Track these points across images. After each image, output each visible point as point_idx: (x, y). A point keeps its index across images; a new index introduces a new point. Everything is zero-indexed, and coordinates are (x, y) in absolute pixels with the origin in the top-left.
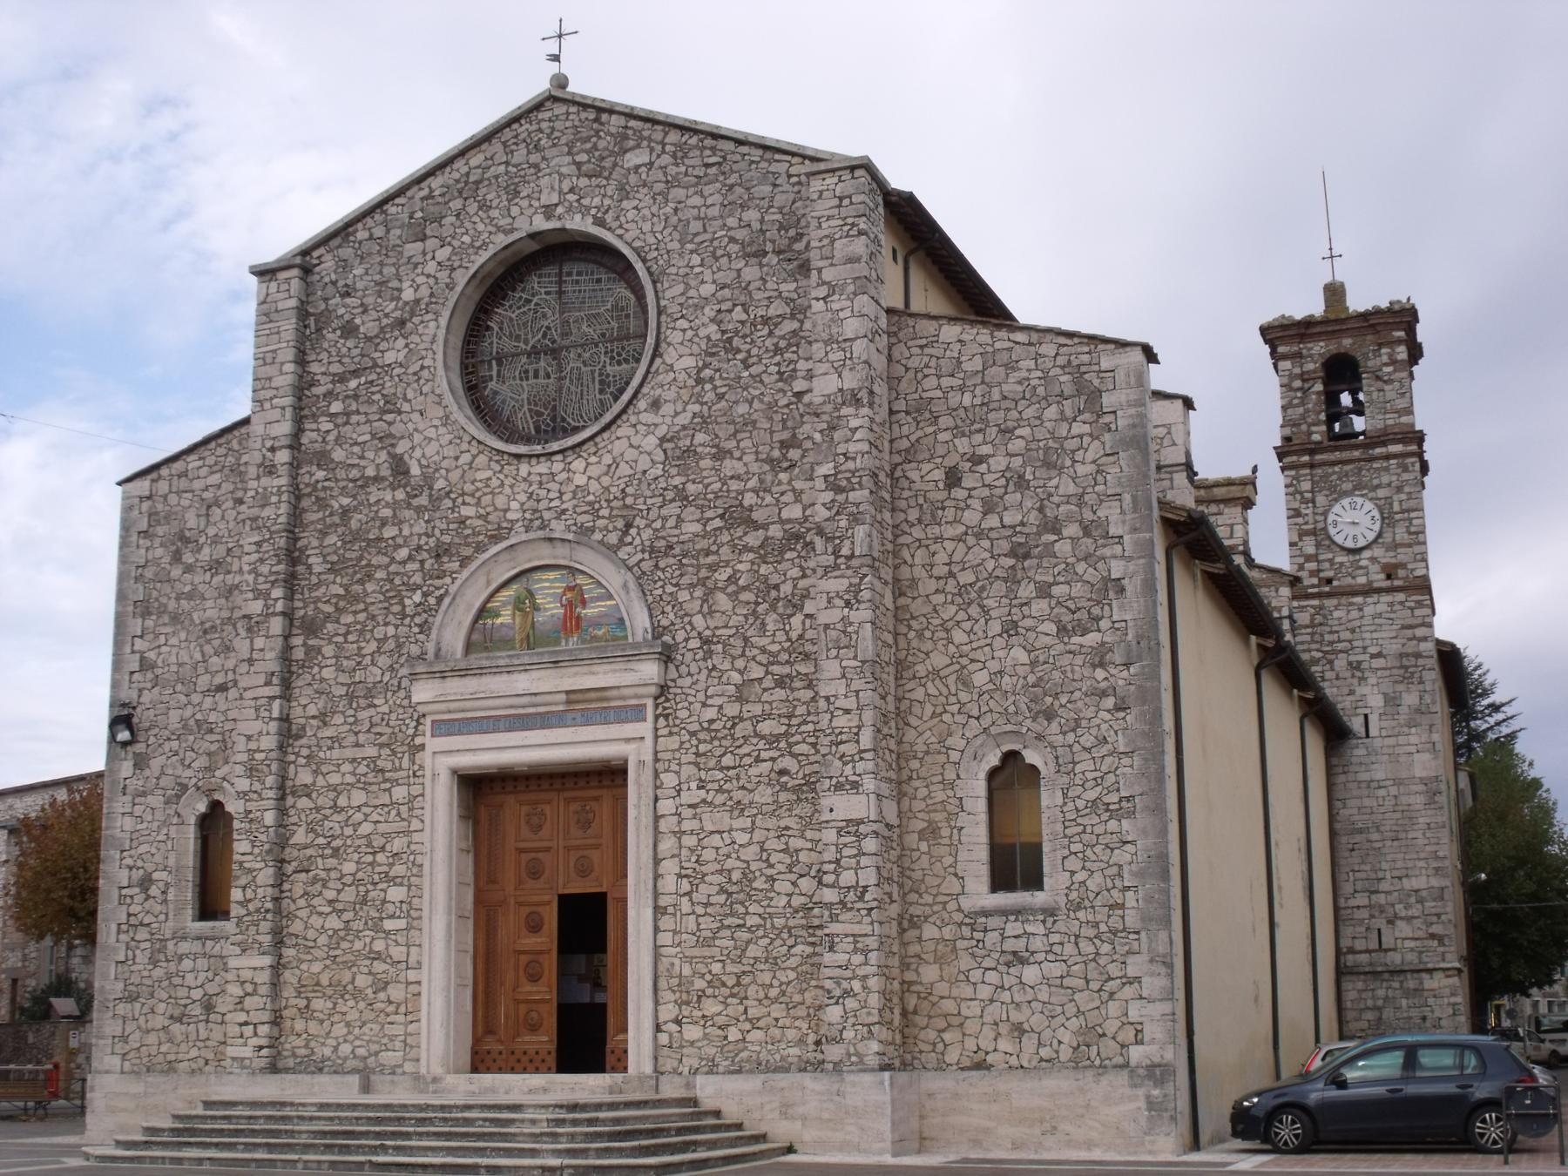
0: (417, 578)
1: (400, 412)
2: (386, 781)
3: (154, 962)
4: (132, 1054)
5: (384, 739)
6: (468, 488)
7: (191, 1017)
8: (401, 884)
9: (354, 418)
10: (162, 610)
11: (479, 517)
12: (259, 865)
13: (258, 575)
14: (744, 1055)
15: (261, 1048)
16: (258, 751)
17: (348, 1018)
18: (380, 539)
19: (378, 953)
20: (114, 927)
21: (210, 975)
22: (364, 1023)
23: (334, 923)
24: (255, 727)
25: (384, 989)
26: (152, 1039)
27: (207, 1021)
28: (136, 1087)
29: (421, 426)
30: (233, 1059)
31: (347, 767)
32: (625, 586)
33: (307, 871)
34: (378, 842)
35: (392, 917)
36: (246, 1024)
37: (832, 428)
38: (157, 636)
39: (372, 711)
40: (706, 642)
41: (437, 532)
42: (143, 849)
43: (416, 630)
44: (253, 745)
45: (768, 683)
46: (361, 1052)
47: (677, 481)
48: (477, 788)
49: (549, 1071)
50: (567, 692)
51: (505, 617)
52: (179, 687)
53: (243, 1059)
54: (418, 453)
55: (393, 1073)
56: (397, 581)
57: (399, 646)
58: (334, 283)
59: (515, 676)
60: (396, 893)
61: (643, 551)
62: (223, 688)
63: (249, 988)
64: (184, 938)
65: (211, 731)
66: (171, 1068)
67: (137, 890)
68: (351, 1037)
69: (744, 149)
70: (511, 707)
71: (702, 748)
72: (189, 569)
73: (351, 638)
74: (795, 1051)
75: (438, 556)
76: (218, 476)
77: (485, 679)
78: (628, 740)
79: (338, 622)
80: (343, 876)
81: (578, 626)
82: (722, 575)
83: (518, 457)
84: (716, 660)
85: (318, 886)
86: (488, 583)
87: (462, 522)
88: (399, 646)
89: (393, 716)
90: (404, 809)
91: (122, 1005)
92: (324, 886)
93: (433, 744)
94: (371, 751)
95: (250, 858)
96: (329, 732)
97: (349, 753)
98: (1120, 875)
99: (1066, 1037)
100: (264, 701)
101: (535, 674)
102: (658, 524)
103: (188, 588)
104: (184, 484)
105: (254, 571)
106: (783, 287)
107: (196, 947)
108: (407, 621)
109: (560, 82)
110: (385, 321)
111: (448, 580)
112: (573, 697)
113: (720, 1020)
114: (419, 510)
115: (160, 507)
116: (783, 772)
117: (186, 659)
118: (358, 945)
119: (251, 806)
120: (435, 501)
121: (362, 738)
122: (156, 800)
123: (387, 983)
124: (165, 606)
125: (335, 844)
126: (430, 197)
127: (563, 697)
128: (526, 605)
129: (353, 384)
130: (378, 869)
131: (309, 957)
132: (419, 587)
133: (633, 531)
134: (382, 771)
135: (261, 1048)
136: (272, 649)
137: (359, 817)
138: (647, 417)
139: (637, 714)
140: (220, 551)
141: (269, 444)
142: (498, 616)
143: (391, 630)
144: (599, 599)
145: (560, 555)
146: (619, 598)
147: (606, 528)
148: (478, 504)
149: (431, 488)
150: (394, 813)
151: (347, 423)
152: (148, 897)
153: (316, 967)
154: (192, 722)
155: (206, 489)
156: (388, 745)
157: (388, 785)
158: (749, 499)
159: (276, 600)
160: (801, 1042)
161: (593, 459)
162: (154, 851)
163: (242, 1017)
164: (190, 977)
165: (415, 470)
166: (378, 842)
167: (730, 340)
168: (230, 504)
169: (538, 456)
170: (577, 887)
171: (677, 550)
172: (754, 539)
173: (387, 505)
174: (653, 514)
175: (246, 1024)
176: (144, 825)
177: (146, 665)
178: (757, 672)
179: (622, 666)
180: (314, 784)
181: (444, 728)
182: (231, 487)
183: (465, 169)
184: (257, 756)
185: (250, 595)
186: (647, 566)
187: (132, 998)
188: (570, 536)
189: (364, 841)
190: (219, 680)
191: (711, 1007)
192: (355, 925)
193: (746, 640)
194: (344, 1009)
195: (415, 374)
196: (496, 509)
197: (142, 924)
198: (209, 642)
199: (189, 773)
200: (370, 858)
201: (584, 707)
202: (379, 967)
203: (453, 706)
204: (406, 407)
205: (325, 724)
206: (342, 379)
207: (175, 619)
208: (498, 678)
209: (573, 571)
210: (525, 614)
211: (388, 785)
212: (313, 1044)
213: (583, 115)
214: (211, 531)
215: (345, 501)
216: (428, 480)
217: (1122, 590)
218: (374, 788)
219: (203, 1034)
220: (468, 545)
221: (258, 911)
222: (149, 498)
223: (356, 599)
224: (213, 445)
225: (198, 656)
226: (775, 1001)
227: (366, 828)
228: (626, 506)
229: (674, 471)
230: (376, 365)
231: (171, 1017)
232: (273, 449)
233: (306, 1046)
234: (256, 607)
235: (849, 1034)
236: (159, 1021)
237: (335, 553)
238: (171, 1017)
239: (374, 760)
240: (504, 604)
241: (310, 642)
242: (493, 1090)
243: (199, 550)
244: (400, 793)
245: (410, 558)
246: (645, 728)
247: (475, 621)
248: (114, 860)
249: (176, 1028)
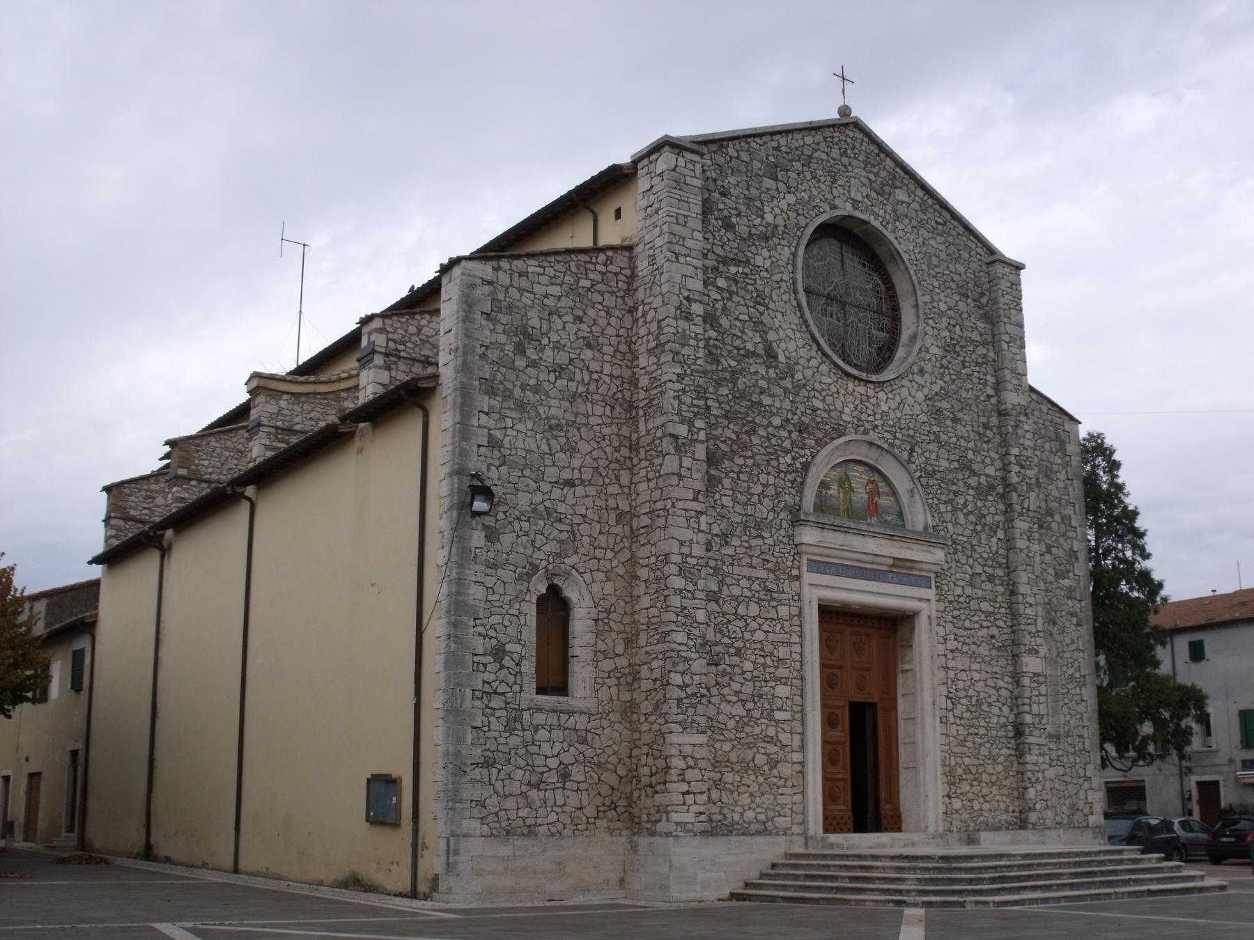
0: (787, 444)
1: (768, 308)
2: (773, 599)
3: (509, 729)
4: (491, 818)
5: (770, 565)
6: (817, 386)
7: (548, 784)
8: (786, 684)
9: (736, 298)
10: (507, 395)
11: (825, 411)
12: (694, 656)
13: (681, 403)
14: (981, 819)
15: (701, 813)
16: (690, 555)
17: (751, 789)
18: (760, 403)
19: (772, 738)
20: (469, 693)
21: (565, 745)
22: (763, 794)
23: (739, 710)
24: (687, 534)
25: (775, 767)
26: (510, 803)
27: (564, 788)
28: (506, 851)
29: (784, 325)
30: (677, 824)
31: (744, 583)
33: (716, 665)
34: (768, 648)
35: (780, 709)
36: (688, 793)
37: (1017, 426)
38: (503, 418)
39: (760, 542)
40: (954, 543)
41: (798, 412)
42: (495, 619)
44: (686, 550)
45: (984, 578)
46: (762, 817)
47: (935, 429)
48: (830, 614)
49: (849, 831)
50: (895, 559)
52: (527, 472)
53: (686, 823)
54: (783, 345)
55: (785, 834)
56: (774, 441)
57: (778, 494)
58: (715, 180)
60: (782, 691)
62: (570, 483)
63: (691, 763)
64: (539, 709)
65: (560, 521)
66: (531, 832)
67: (490, 659)
68: (753, 806)
69: (955, 223)
70: (859, 561)
71: (956, 613)
72: (533, 364)
73: (742, 477)
74: (1004, 817)
75: (800, 431)
76: (558, 288)
77: (849, 537)
78: (920, 600)
79: (732, 460)
80: (744, 672)
82: (961, 500)
83: (848, 375)
84: (959, 556)
85: (727, 678)
88: (778, 494)
89: (777, 549)
90: (787, 624)
91: (477, 770)
92: (731, 679)
93: (808, 578)
94: (762, 574)
95: (684, 648)
96: (730, 551)
97: (747, 571)
98: (1081, 719)
99: (1065, 810)
100: (693, 514)
101: (879, 541)
103: (533, 382)
104: (524, 283)
105: (677, 398)
106: (979, 324)
107: (552, 719)
108: (782, 475)
109: (844, 111)
110: (754, 231)
112: (897, 563)
113: (970, 796)
114: (786, 390)
115: (501, 296)
116: (993, 637)
117: (534, 447)
118: (757, 730)
119: (686, 603)
120: (798, 387)
121: (755, 562)
122: (507, 575)
123: (777, 762)
124: (511, 392)
125: (736, 645)
126: (777, 149)
127: (891, 561)
129: (733, 269)
130: (768, 670)
131: (722, 738)
134: (769, 591)
135: (701, 813)
136: (698, 471)
137: (754, 625)
138: (918, 378)
139: (924, 582)
140: (563, 358)
141: (686, 294)
143: (771, 480)
146: (905, 498)
148: (823, 401)
149: (792, 377)
150: (779, 626)
151: (730, 299)
152: (502, 667)
153: (727, 747)
154: (541, 508)
155: (546, 296)
156: (773, 571)
157: (775, 603)
158: (970, 455)
159: (699, 429)
160: (1007, 811)
161: (890, 395)
162: (506, 623)
163: (685, 787)
164: (546, 748)
165: (782, 358)
166: (768, 648)
167: (955, 345)
168: (569, 318)
169: (860, 380)
170: (859, 697)
171: (938, 476)
172: (973, 481)
173: (763, 378)
175: (688, 793)
176: (496, 597)
177: (493, 444)
178: (979, 570)
179: (926, 548)
180: (720, 590)
181: (818, 566)
182: (571, 304)
183: (801, 143)
184: (689, 560)
185: (676, 418)
187: (488, 764)
189: (759, 646)
190: (566, 475)
191: (965, 787)
192: (756, 714)
193: (972, 546)
194: (749, 782)
195: (777, 282)
197: (495, 692)
198: (555, 437)
199: (538, 555)
200: (761, 660)
201: (900, 571)
202: (772, 749)
204: (772, 305)
205: (727, 543)
206: (725, 261)
207: (521, 406)
208: (856, 538)
209: (875, 470)
210: (846, 493)
211: (775, 603)
212: (725, 811)
213: (872, 147)
214: (555, 338)
215: (734, 364)
216: (790, 372)
217: (1077, 559)
218: (766, 604)
219: (560, 801)
220: (820, 429)
221: (695, 695)
222: (490, 283)
223: (745, 447)
224: (552, 259)
225: (545, 448)
226: (994, 784)
227: (759, 635)
229: (933, 421)
230: (748, 262)
231: (529, 784)
232: (687, 299)
233: (720, 813)
234: (682, 430)
235: (1038, 806)
236: (516, 788)
237: (727, 403)
238: (529, 784)
239: (765, 580)
240: (833, 480)
241: (712, 472)
242: (883, 845)
243: (542, 350)
244: (784, 611)
245: (782, 426)
246: (931, 593)
248: (467, 626)
249: (533, 793)
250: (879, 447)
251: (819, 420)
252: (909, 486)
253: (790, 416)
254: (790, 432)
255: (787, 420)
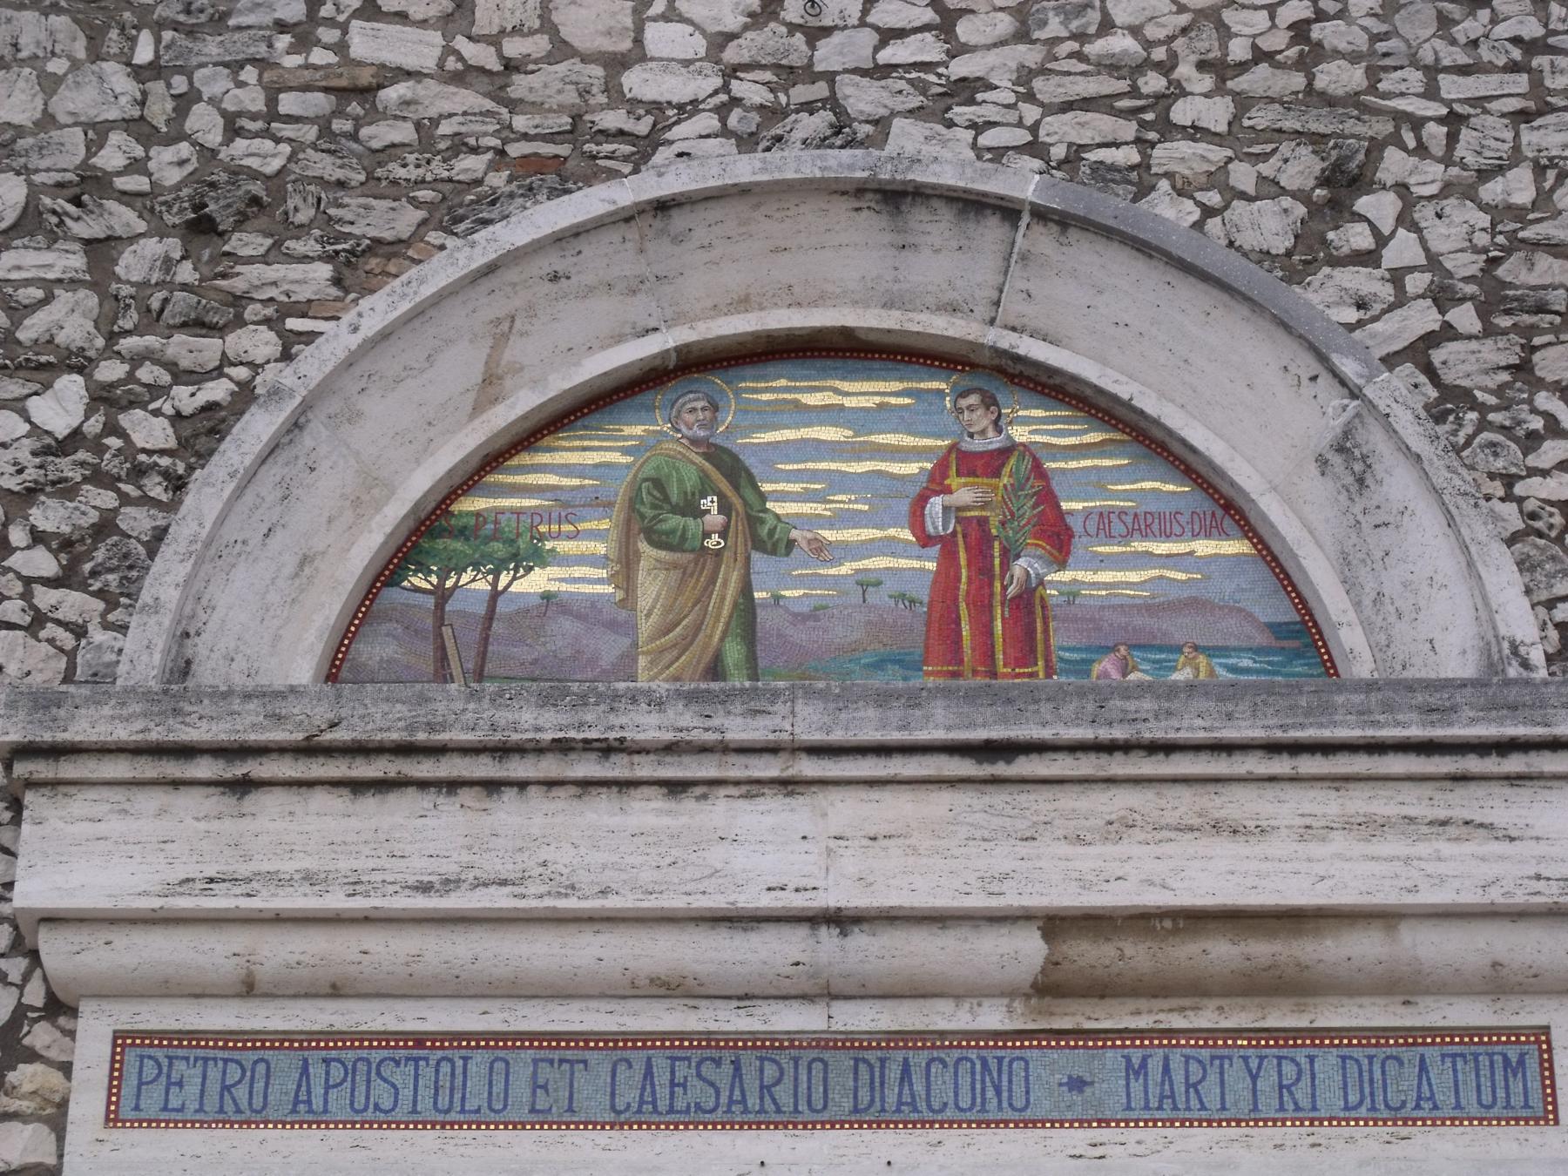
0: (70, 320)
11: (465, 75)
32: (1347, 457)
43: (43, 563)
50: (1055, 924)
51: (573, 570)
59: (720, 812)
61: (1442, 297)
70: (668, 988)
75: (201, 227)
77: (510, 816)
81: (1026, 646)
86: (490, 387)
87: (359, 91)
101: (845, 809)
102: (1519, 187)
111: (258, 342)
112: (1088, 953)
127: (1030, 948)
128: (704, 520)
132: (78, 362)
133: (1379, 206)
142: (527, 556)
144: (1144, 524)
145: (938, 285)
147: (1217, 178)
174: (1485, 138)
186: (1472, 362)
188: (1024, 182)
196: (562, 50)
203: (279, 951)
208: (601, 812)
210: (698, 562)
220: (398, 190)
228: (1314, 97)
240: (567, 507)
247: (390, 570)
250: (971, 205)
251: (381, 134)
252: (1321, 415)
253: (111, 157)
254: (101, 249)
255: (89, 186)
